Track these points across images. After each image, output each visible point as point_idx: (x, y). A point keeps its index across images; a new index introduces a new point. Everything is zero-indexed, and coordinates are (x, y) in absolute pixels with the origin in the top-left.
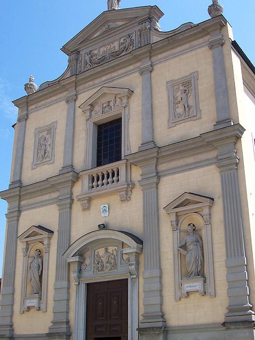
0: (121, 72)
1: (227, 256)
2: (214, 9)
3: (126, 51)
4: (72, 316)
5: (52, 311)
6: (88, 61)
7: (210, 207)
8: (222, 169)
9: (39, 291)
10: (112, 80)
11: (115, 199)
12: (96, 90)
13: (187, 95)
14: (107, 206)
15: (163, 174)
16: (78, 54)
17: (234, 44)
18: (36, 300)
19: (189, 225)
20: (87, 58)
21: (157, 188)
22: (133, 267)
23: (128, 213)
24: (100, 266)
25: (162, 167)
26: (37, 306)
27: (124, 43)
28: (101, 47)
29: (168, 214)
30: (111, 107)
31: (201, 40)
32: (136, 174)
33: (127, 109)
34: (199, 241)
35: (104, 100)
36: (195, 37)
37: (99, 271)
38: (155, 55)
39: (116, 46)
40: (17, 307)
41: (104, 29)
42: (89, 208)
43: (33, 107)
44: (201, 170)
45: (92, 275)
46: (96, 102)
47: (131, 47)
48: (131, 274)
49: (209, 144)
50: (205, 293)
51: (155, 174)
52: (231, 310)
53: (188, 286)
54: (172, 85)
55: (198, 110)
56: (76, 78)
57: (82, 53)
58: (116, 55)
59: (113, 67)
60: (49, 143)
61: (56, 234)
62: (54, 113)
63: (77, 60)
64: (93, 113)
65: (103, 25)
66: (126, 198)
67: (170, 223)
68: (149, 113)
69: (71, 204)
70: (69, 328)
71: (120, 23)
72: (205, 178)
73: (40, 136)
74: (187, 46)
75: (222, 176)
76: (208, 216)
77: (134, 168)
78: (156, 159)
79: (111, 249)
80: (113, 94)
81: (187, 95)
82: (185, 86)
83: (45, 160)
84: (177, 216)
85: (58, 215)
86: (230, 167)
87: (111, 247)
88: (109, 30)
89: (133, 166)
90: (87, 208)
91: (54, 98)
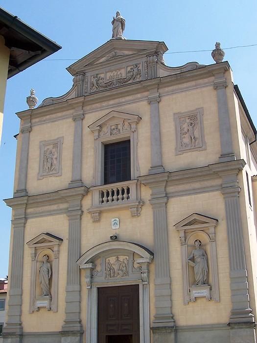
0: (128, 98)
1: (231, 270)
2: (217, 53)
4: (84, 316)
5: (64, 310)
6: (95, 84)
7: (215, 227)
8: (226, 195)
10: (120, 104)
11: (127, 213)
14: (118, 220)
16: (84, 75)
17: (236, 87)
18: (47, 302)
19: (196, 241)
20: (94, 81)
21: (166, 207)
22: (145, 275)
24: (111, 272)
25: (170, 189)
27: (131, 72)
28: (109, 72)
29: (178, 231)
30: (119, 130)
31: (206, 80)
32: (146, 193)
33: (135, 133)
34: (205, 255)
35: (113, 123)
36: (201, 76)
37: (111, 277)
38: (162, 88)
39: (123, 73)
40: (26, 307)
41: (111, 55)
43: (37, 120)
44: (206, 194)
45: (103, 281)
46: (104, 124)
49: (216, 173)
51: (164, 195)
52: (234, 313)
53: (196, 293)
54: (179, 117)
55: (203, 142)
56: (84, 99)
57: (87, 74)
58: (123, 82)
59: (121, 93)
60: (55, 157)
61: (66, 242)
65: (110, 52)
66: (136, 214)
67: (178, 238)
68: (157, 139)
69: (81, 216)
70: (81, 326)
71: (127, 53)
72: (211, 202)
73: (45, 149)
74: (193, 83)
77: (143, 188)
79: (121, 258)
80: (123, 118)
81: (193, 127)
82: (191, 120)
83: (51, 173)
84: (185, 232)
87: (121, 256)
88: (115, 57)
89: (142, 185)
90: (97, 220)
91: (59, 115)
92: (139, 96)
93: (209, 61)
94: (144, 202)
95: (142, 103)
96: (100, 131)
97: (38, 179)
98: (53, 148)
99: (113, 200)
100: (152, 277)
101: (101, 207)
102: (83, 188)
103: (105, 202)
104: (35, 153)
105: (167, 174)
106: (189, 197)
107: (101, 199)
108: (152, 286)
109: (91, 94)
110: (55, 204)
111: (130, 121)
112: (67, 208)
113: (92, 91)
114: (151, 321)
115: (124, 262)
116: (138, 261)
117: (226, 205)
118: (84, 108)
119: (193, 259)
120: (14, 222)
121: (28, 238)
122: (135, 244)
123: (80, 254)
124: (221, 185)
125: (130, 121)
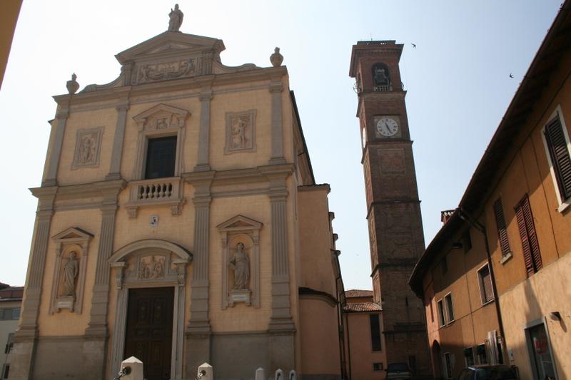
1: (273, 274)
2: (277, 58)
3: (187, 73)
5: (89, 311)
7: (260, 230)
8: (273, 199)
9: (72, 293)
12: (151, 105)
17: (292, 93)
18: (70, 302)
20: (144, 72)
21: (210, 208)
22: (183, 276)
23: (181, 227)
24: (145, 273)
25: (215, 189)
26: (71, 308)
28: (161, 64)
29: (220, 232)
30: (166, 125)
31: (262, 83)
32: (190, 192)
34: (246, 259)
39: (176, 67)
40: (45, 308)
42: (137, 217)
43: (77, 106)
44: (253, 197)
45: (135, 281)
47: (192, 72)
48: (179, 283)
53: (235, 297)
54: (230, 118)
57: (138, 65)
58: (175, 76)
59: (172, 87)
60: (93, 146)
61: (97, 238)
62: (106, 118)
64: (147, 127)
68: (207, 138)
70: (108, 330)
71: (182, 46)
73: (83, 138)
74: (248, 84)
75: (272, 205)
76: (257, 238)
77: (187, 186)
79: (158, 258)
83: (87, 163)
85: (101, 220)
86: (280, 199)
92: (191, 91)
93: (265, 63)
94: (186, 201)
96: (145, 124)
97: (72, 170)
98: (92, 137)
99: (153, 197)
100: (190, 279)
102: (121, 181)
103: (144, 199)
104: (71, 141)
107: (140, 195)
108: (189, 290)
109: (139, 84)
111: (178, 116)
112: (102, 202)
113: (141, 82)
115: (160, 262)
116: (175, 262)
119: (234, 262)
120: (40, 213)
121: (54, 232)
123: (112, 251)
125: (178, 116)
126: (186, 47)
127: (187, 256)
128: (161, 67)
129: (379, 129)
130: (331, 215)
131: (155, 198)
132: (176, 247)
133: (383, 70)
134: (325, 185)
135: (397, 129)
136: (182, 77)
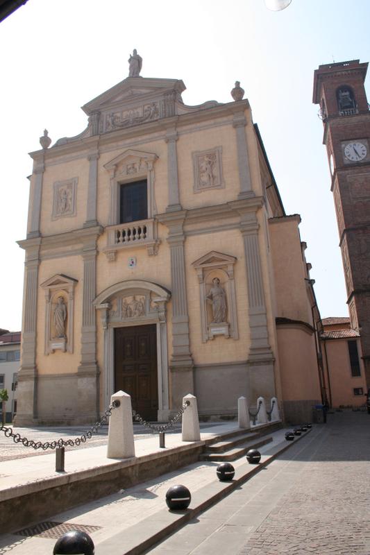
2: (238, 91)
3: (151, 118)
4: (101, 357)
6: (111, 123)
7: (234, 265)
8: (245, 233)
9: (63, 335)
12: (119, 152)
13: (211, 166)
15: (189, 233)
17: (256, 126)
21: (184, 246)
23: (158, 267)
24: (128, 312)
25: (188, 228)
26: (63, 348)
28: (125, 111)
29: (196, 269)
30: (136, 169)
31: (225, 119)
32: (163, 232)
33: (153, 172)
34: (223, 293)
39: (140, 112)
41: (127, 94)
42: (115, 260)
43: (50, 160)
44: (225, 233)
45: (120, 321)
47: (156, 115)
48: (160, 320)
49: (235, 211)
50: (230, 337)
51: (182, 234)
53: (214, 331)
54: (197, 156)
57: (104, 114)
58: (139, 121)
60: (70, 197)
61: (81, 283)
63: (98, 120)
64: (118, 173)
68: (176, 178)
69: (96, 256)
70: (98, 367)
71: (144, 91)
74: (212, 122)
77: (160, 227)
78: (183, 220)
81: (211, 166)
83: (65, 214)
85: (83, 266)
91: (74, 154)
92: (156, 134)
93: (227, 98)
94: (161, 242)
95: (159, 142)
96: (115, 171)
97: (52, 221)
98: (68, 188)
99: (129, 240)
100: (170, 315)
101: (116, 247)
102: (98, 228)
103: (121, 243)
104: (49, 194)
105: (184, 212)
106: (207, 235)
107: (117, 239)
108: (170, 326)
109: (106, 133)
110: (70, 245)
112: (82, 249)
113: (108, 130)
114: (169, 359)
115: (141, 302)
117: (245, 243)
118: (100, 147)
119: (211, 297)
120: (28, 263)
121: (42, 280)
122: (153, 283)
124: (240, 223)
126: (148, 91)
127: (165, 294)
128: (125, 113)
129: (347, 155)
130: (303, 245)
131: (131, 241)
132: (151, 284)
133: (347, 93)
134: (295, 215)
135: (365, 153)
136: (147, 121)
